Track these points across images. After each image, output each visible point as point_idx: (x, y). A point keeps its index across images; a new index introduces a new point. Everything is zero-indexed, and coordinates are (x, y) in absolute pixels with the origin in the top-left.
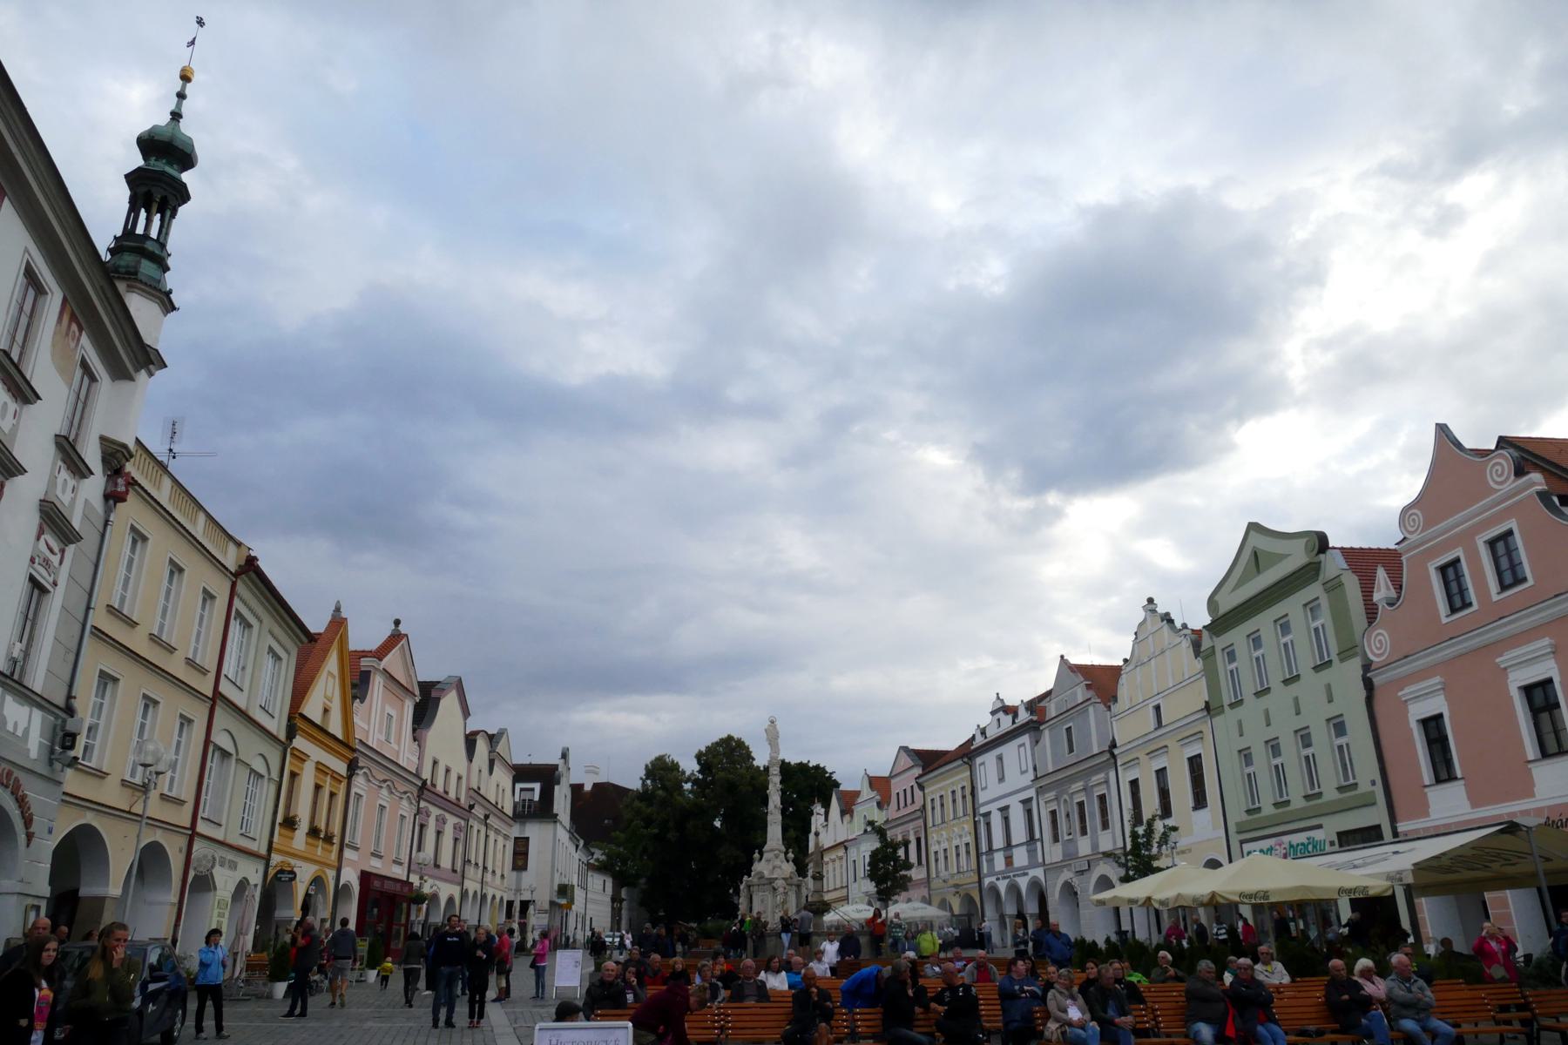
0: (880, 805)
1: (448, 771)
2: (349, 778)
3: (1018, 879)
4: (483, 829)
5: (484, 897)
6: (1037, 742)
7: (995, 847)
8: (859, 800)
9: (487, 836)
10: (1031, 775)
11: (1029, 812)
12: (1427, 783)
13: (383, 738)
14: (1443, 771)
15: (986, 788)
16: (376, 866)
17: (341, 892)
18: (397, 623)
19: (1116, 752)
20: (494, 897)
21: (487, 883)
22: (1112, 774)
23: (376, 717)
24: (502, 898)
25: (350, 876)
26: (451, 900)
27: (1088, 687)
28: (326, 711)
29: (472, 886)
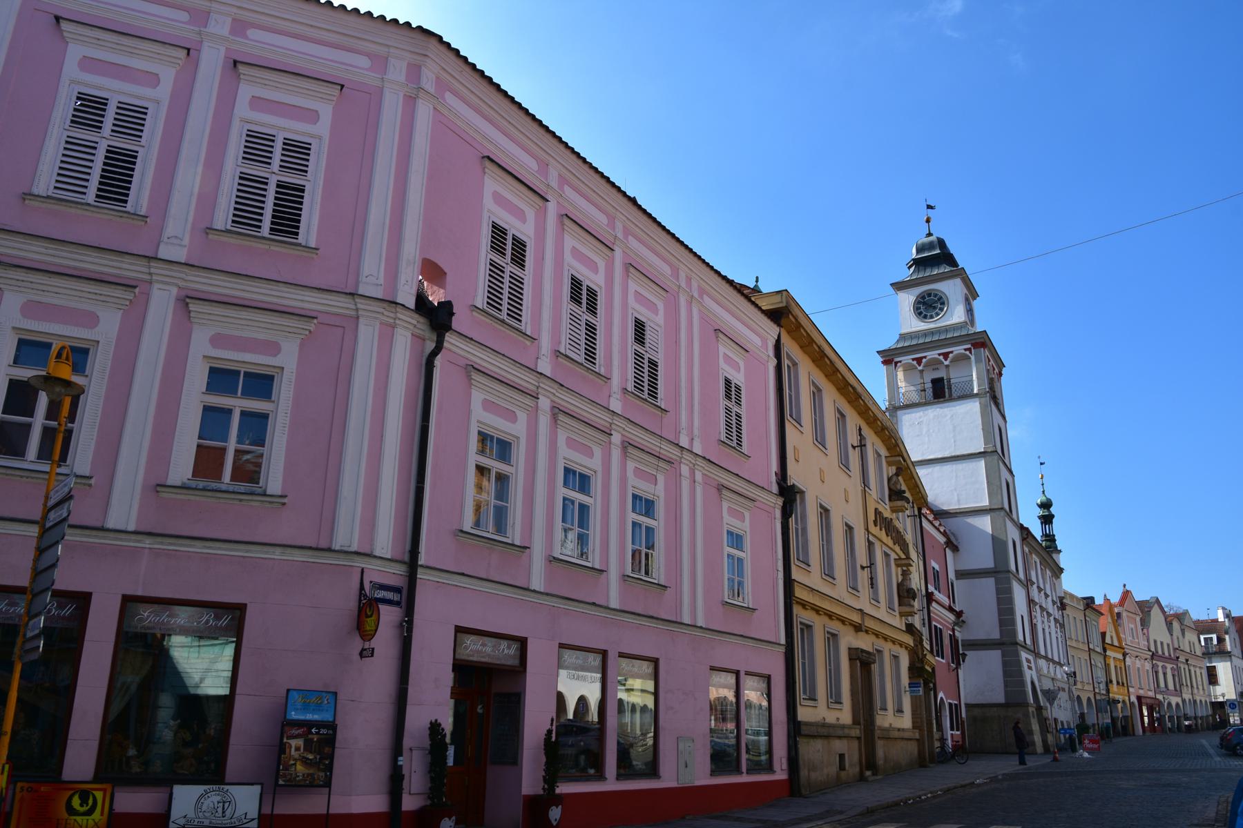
1: (1162, 643)
2: (1124, 659)
4: (1186, 666)
5: (1195, 701)
9: (1189, 670)
13: (1131, 638)
16: (1141, 692)
17: (1132, 704)
18: (1125, 586)
20: (1201, 701)
21: (1195, 694)
25: (1133, 699)
26: (1177, 704)
29: (1187, 696)
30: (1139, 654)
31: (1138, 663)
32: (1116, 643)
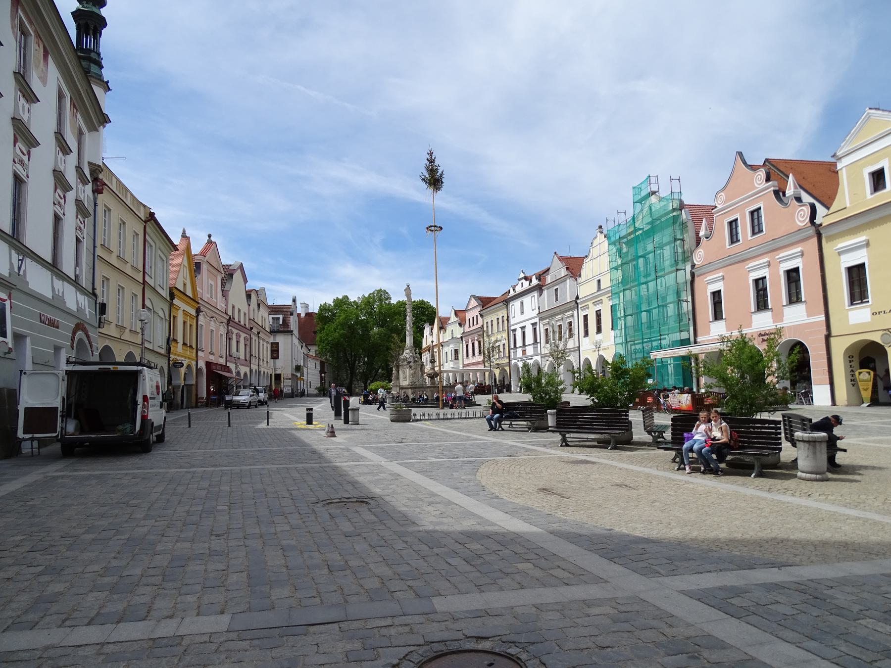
0: (460, 325)
1: (239, 311)
2: (197, 317)
3: (528, 361)
5: (260, 372)
6: (541, 295)
7: (517, 346)
8: (449, 322)
9: (259, 342)
10: (537, 311)
11: (535, 329)
12: (711, 320)
13: (209, 296)
14: (718, 315)
15: (514, 317)
16: (212, 359)
17: (199, 371)
18: (210, 236)
19: (578, 301)
20: (264, 372)
22: (576, 312)
23: (205, 287)
24: (268, 373)
25: (202, 364)
26: (245, 374)
27: (567, 269)
28: (185, 285)
29: (254, 367)
30: (215, 315)
31: (213, 325)
32: (189, 293)
